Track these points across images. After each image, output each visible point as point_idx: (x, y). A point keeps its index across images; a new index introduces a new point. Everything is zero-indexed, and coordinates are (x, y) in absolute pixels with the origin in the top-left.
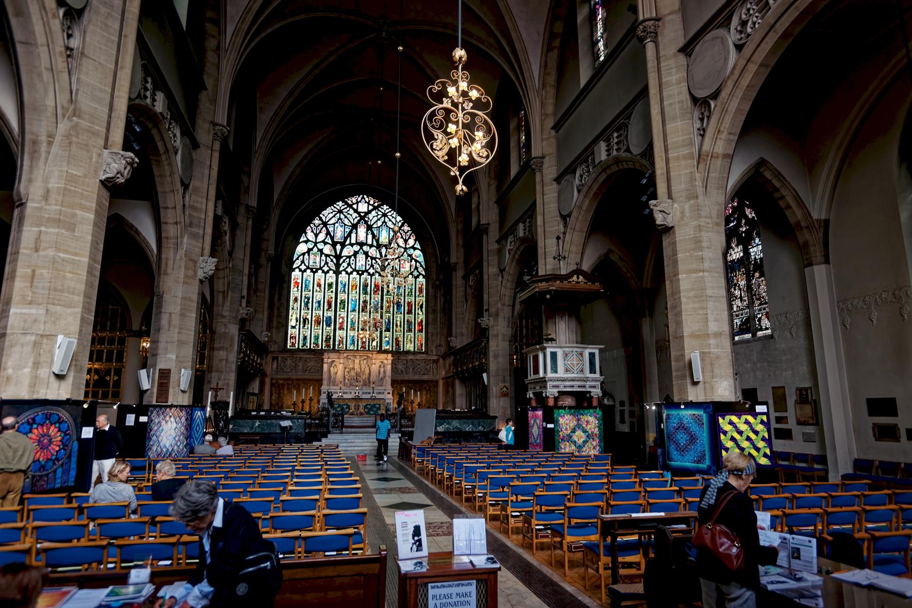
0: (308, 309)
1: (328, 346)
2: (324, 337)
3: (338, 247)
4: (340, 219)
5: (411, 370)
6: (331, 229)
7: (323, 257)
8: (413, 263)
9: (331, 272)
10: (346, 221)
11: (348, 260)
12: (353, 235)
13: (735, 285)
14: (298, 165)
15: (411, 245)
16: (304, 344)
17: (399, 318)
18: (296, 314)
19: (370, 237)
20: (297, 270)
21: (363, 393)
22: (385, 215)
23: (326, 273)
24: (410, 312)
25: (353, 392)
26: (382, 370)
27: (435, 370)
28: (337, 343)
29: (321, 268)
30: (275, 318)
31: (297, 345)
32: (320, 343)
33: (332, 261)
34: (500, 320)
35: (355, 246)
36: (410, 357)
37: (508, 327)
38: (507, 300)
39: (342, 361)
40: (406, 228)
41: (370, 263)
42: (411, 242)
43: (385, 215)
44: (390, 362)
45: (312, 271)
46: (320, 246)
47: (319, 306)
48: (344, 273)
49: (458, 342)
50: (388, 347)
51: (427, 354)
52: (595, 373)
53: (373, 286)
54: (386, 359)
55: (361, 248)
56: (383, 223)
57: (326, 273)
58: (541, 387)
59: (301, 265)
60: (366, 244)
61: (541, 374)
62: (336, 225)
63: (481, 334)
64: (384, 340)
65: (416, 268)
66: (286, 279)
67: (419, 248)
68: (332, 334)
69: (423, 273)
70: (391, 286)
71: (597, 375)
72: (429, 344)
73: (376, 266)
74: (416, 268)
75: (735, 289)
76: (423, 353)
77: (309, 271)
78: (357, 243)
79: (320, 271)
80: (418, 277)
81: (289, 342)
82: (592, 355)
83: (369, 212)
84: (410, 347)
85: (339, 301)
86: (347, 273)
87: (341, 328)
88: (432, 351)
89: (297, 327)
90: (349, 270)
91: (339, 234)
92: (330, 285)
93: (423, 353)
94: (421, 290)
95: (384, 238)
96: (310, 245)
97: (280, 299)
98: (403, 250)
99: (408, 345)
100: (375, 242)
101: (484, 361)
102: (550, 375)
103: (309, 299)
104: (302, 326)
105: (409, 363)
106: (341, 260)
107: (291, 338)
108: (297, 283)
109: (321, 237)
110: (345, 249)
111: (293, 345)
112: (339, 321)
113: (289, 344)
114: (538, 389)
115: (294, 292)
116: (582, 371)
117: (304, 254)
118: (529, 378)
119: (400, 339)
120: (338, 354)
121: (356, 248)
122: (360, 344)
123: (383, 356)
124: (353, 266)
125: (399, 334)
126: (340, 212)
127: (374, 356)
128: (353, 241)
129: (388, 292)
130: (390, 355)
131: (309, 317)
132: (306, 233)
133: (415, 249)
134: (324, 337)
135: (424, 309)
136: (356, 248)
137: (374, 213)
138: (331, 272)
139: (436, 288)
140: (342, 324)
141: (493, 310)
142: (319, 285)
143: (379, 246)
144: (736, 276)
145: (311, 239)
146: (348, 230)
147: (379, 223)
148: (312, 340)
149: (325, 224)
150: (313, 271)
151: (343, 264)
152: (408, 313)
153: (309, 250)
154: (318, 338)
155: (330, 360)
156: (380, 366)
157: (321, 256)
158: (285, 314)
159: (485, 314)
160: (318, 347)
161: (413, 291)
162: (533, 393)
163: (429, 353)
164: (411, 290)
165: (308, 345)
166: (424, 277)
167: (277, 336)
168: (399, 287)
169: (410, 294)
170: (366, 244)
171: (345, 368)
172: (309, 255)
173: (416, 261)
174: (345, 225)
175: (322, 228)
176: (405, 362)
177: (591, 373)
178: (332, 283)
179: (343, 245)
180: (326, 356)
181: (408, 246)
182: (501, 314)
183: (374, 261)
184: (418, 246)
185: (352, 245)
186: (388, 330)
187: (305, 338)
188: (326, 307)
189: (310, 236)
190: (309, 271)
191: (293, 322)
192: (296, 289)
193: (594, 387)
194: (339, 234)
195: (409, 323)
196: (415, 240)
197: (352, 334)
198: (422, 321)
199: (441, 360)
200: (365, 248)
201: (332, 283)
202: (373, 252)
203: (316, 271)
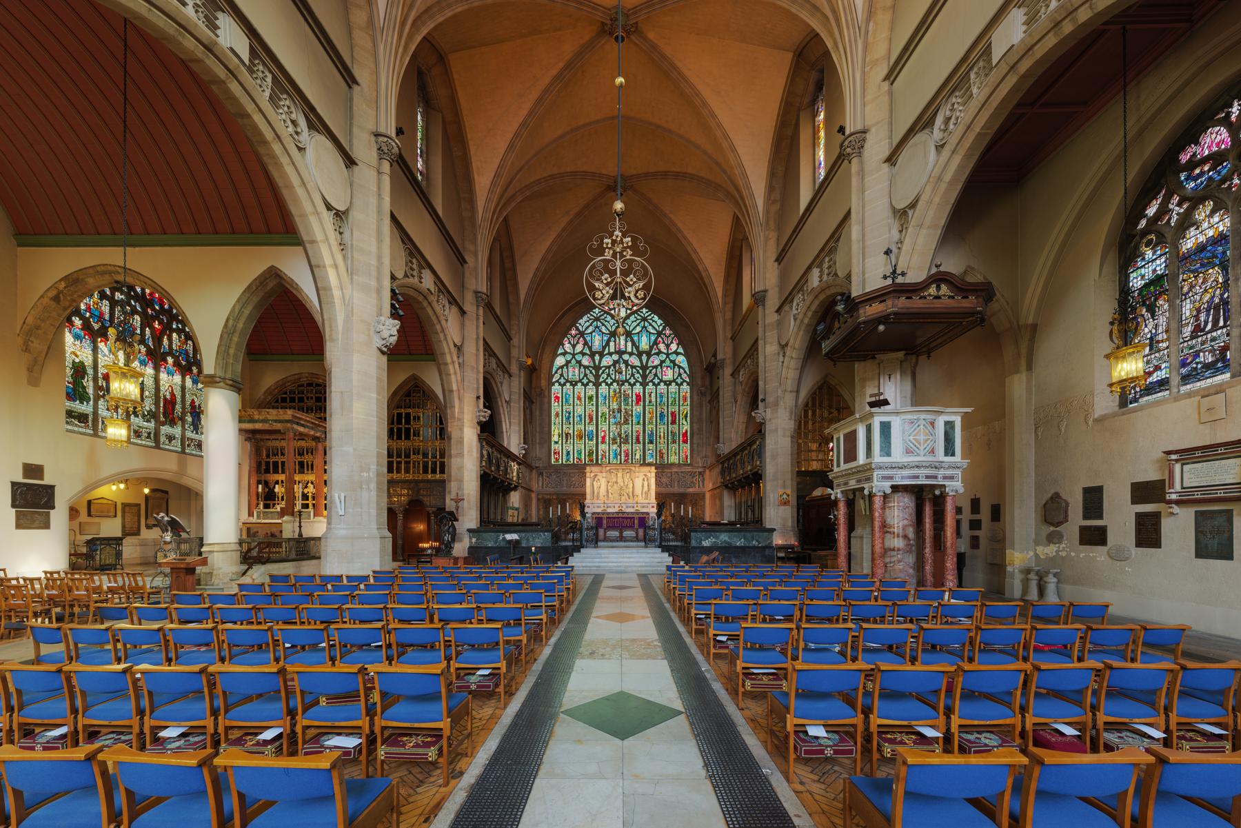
0: (570, 423)
1: (592, 461)
3: (597, 357)
4: (597, 327)
5: (676, 483)
6: (588, 339)
7: (582, 369)
8: (676, 369)
9: (591, 384)
10: (604, 330)
11: (607, 370)
12: (612, 344)
14: (543, 259)
15: (673, 350)
17: (662, 429)
18: (558, 429)
19: (629, 344)
20: (557, 384)
21: (627, 507)
22: (644, 319)
23: (585, 385)
24: (673, 422)
25: (617, 506)
26: (646, 483)
28: (600, 457)
29: (580, 381)
30: (537, 434)
33: (591, 372)
34: (779, 410)
35: (614, 356)
36: (675, 470)
37: (790, 419)
38: (790, 384)
39: (604, 474)
40: (668, 332)
41: (630, 372)
42: (674, 347)
43: (644, 319)
44: (653, 475)
45: (571, 384)
46: (578, 357)
47: (581, 420)
48: (603, 384)
49: (725, 448)
53: (634, 396)
55: (620, 357)
56: (643, 328)
57: (585, 385)
58: (859, 481)
59: (560, 378)
60: (625, 352)
61: (861, 458)
62: (594, 334)
63: (758, 431)
64: (647, 452)
65: (680, 375)
66: (546, 393)
67: (682, 351)
69: (688, 380)
70: (653, 395)
72: (695, 456)
73: (637, 375)
74: (680, 375)
76: (688, 465)
77: (568, 384)
78: (616, 352)
79: (579, 384)
80: (682, 384)
82: (949, 426)
83: (628, 317)
84: (673, 459)
85: (600, 415)
86: (607, 384)
87: (603, 442)
89: (560, 442)
90: (609, 381)
91: (597, 343)
92: (591, 398)
94: (685, 399)
95: (644, 344)
96: (569, 357)
97: (541, 414)
98: (665, 356)
100: (634, 349)
101: (758, 463)
102: (878, 458)
103: (570, 413)
104: (564, 441)
105: (673, 476)
106: (601, 371)
108: (557, 398)
109: (579, 348)
110: (604, 359)
111: (557, 460)
112: (601, 434)
114: (853, 484)
115: (555, 407)
116: (932, 452)
117: (562, 367)
118: (836, 469)
119: (664, 451)
120: (600, 468)
121: (615, 357)
123: (646, 469)
124: (613, 377)
125: (663, 447)
126: (597, 319)
127: (637, 469)
128: (612, 350)
129: (650, 402)
130: (653, 468)
131: (571, 432)
132: (563, 345)
133: (677, 353)
135: (688, 419)
136: (615, 357)
137: (632, 318)
138: (591, 384)
139: (702, 394)
140: (603, 438)
141: (770, 399)
142: (579, 399)
143: (640, 355)
145: (569, 351)
146: (605, 338)
147: (638, 329)
148: (576, 455)
149: (582, 334)
150: (574, 384)
151: (603, 375)
152: (671, 424)
153: (568, 362)
155: (592, 475)
156: (644, 480)
157: (580, 368)
158: (547, 429)
159: (761, 405)
161: (677, 400)
162: (842, 492)
164: (675, 399)
166: (688, 384)
167: (538, 452)
168: (661, 397)
169: (673, 403)
170: (625, 352)
171: (608, 482)
172: (567, 368)
173: (680, 367)
174: (603, 333)
175: (579, 339)
176: (669, 475)
177: (946, 454)
178: (592, 396)
179: (602, 355)
180: (588, 469)
181: (670, 352)
182: (782, 403)
183: (634, 370)
184: (681, 350)
185: (610, 354)
186: (651, 442)
187: (568, 453)
188: (587, 421)
189: (568, 347)
190: (568, 384)
191: (555, 438)
192: (556, 404)
194: (597, 343)
195: (673, 434)
196: (678, 345)
197: (614, 448)
198: (686, 431)
200: (626, 357)
201: (592, 396)
202: (634, 361)
203: (576, 384)
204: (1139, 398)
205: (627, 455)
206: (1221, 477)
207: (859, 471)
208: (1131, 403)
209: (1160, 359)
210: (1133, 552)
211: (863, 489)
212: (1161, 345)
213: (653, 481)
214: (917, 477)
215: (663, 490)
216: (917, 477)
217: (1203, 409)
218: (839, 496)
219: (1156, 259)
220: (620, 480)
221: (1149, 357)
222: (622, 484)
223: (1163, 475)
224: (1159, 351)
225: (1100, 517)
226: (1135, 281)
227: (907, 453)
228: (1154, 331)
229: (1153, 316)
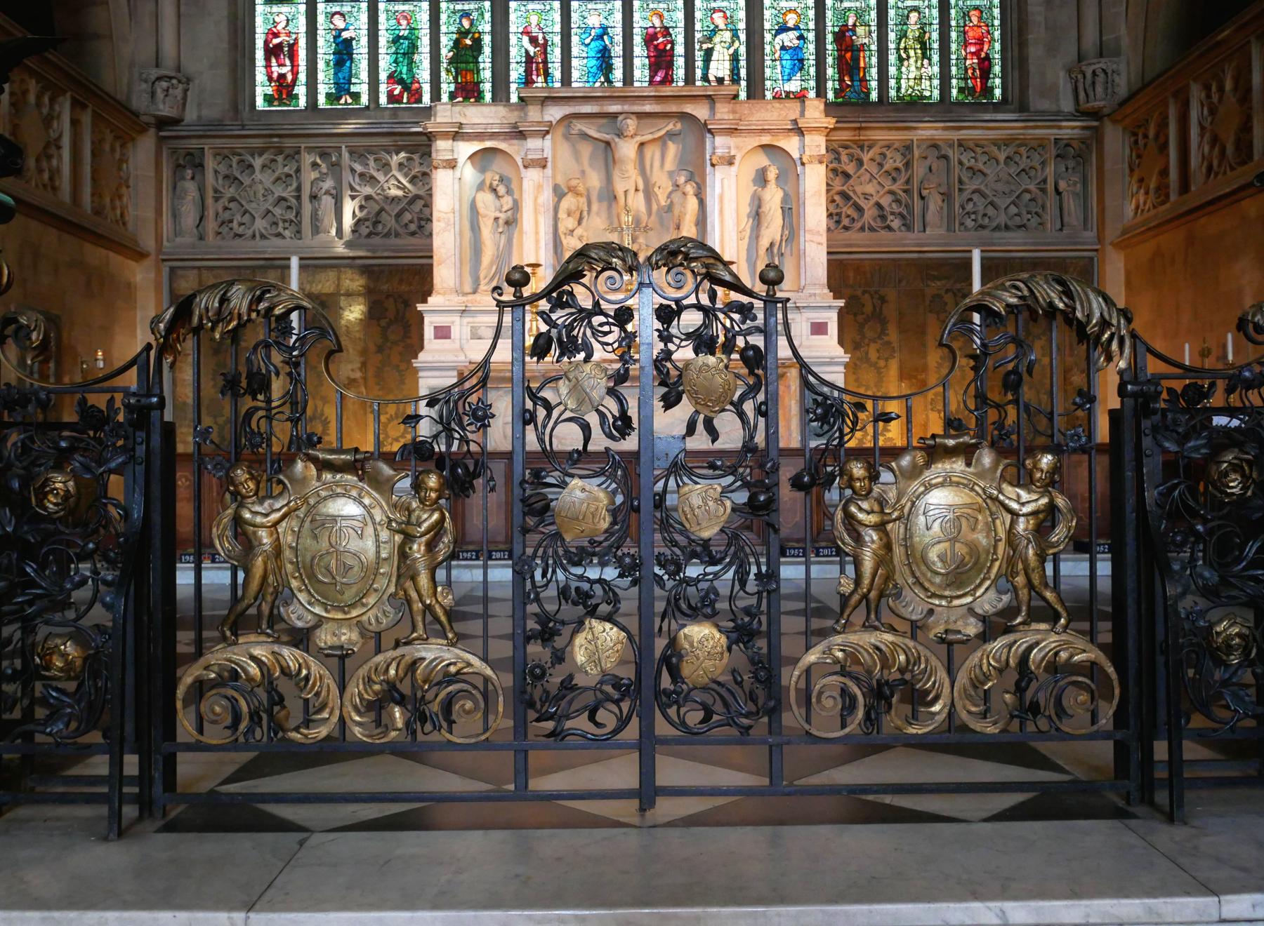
2: (446, 42)
5: (935, 203)
16: (342, 87)
26: (773, 197)
27: (1071, 204)
28: (516, 72)
31: (301, 90)
32: (424, 74)
44: (816, 144)
50: (794, 86)
51: (1023, 107)
54: (800, 132)
64: (772, 44)
68: (486, 27)
72: (1035, 52)
81: (261, 76)
88: (1051, 92)
93: (997, 107)
99: (911, 69)
105: (919, 170)
107: (273, 52)
111: (284, 89)
113: (263, 88)
119: (865, 36)
122: (641, 72)
134: (446, 42)
148: (385, 64)
154: (413, 48)
156: (761, 178)
160: (416, 96)
163: (1038, 103)
165: (363, 89)
176: (894, 161)
187: (344, 50)
197: (594, 21)
199: (1115, 142)
205: (661, 61)
213: (815, 180)
215: (857, 240)
220: (627, 180)
222: (638, 202)
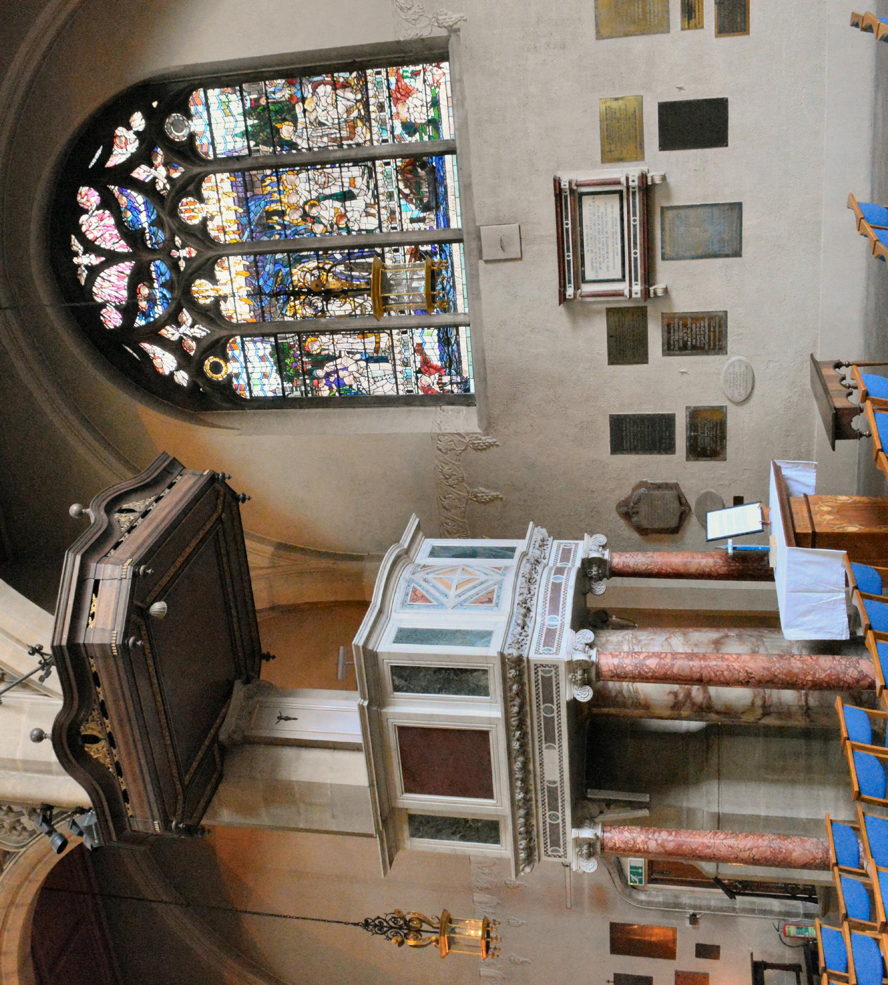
13: (305, 216)
52: (513, 550)
71: (520, 545)
75: (316, 220)
144: (282, 214)
193: (566, 555)
204: (462, 378)
206: (610, 225)
207: (521, 725)
208: (468, 390)
209: (405, 344)
210: (734, 358)
211: (574, 705)
212: (382, 345)
214: (556, 588)
216: (556, 588)
217: (501, 255)
218: (587, 833)
219: (245, 356)
221: (398, 362)
223: (599, 312)
224: (392, 346)
225: (668, 421)
226: (266, 388)
227: (490, 601)
228: (358, 356)
229: (333, 358)
